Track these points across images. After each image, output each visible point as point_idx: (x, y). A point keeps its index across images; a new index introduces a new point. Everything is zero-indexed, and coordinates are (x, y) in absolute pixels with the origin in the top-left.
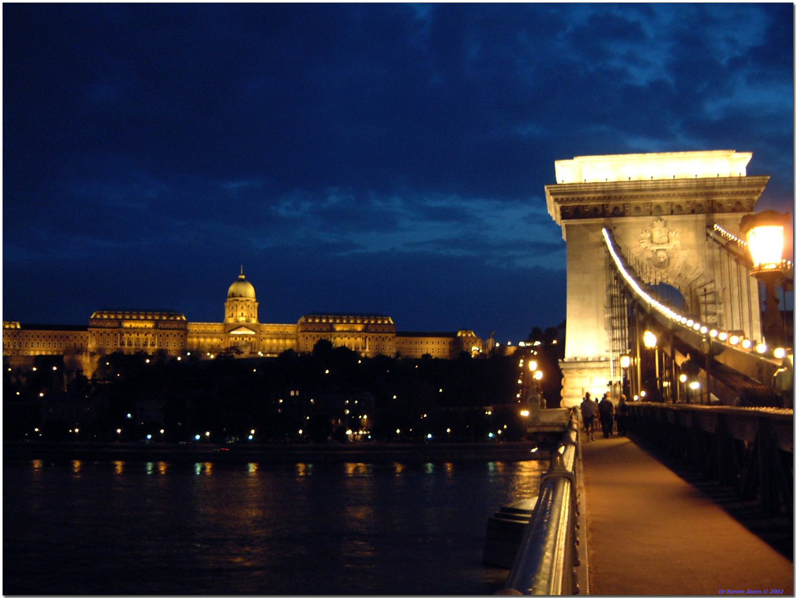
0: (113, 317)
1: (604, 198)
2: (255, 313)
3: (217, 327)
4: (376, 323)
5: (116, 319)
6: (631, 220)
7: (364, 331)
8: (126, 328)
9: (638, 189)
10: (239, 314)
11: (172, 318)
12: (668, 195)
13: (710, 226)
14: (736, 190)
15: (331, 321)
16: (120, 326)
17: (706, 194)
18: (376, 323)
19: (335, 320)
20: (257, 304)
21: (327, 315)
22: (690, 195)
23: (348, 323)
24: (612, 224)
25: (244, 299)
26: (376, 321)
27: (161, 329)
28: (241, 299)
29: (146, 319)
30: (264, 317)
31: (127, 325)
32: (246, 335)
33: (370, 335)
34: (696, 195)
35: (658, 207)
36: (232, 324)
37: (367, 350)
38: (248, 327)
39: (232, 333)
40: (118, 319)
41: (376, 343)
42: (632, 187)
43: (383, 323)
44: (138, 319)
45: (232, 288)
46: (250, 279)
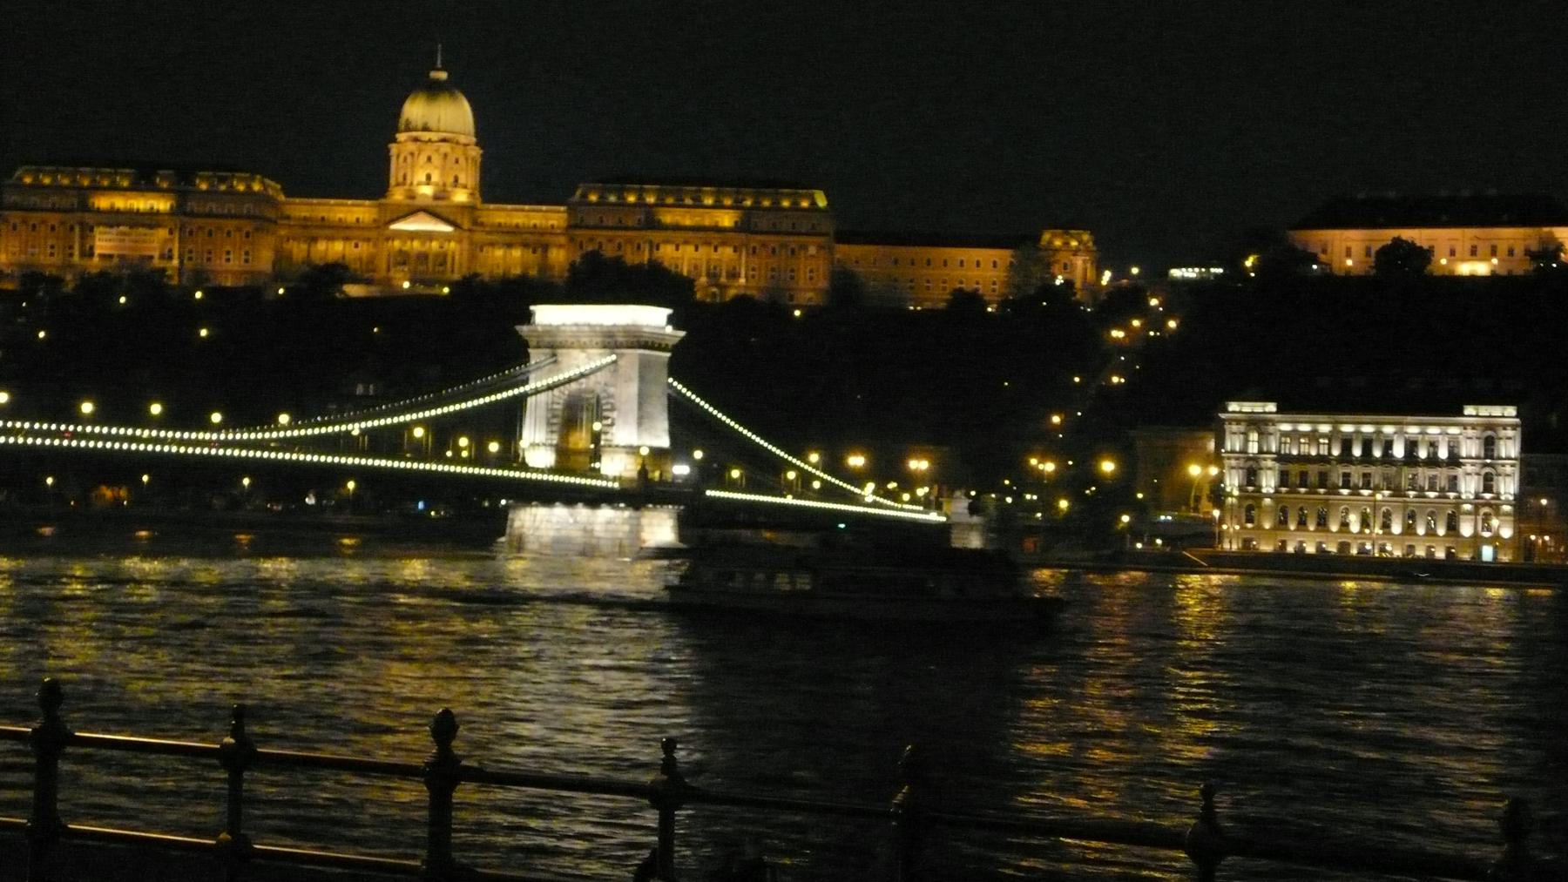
2: (469, 176)
3: (358, 212)
4: (776, 208)
7: (743, 227)
8: (98, 211)
10: (424, 179)
11: (223, 187)
15: (651, 200)
16: (85, 207)
20: (475, 152)
21: (639, 181)
25: (434, 136)
26: (776, 203)
27: (192, 215)
28: (426, 136)
30: (498, 183)
31: (103, 202)
36: (399, 205)
37: (742, 281)
39: (395, 227)
40: (81, 188)
41: (773, 262)
43: (795, 207)
45: (415, 110)
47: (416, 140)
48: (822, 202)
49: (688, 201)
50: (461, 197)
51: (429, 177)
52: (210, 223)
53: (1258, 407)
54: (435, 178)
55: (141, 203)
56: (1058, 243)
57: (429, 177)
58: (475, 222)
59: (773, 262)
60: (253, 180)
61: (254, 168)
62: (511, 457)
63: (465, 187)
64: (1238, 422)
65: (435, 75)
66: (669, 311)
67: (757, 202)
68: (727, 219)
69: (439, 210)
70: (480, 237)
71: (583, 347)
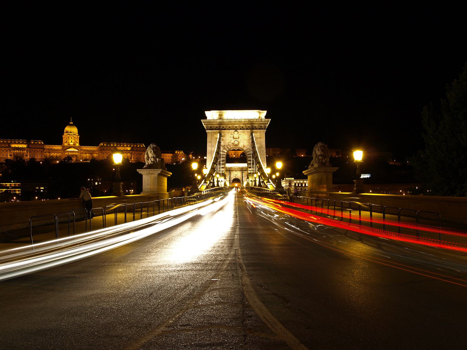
1: (219, 124)
3: (59, 147)
4: (137, 147)
5: (7, 143)
6: (227, 131)
9: (230, 122)
10: (71, 142)
11: (36, 143)
12: (239, 124)
13: (252, 134)
14: (260, 123)
16: (9, 147)
17: (251, 124)
21: (113, 141)
22: (246, 124)
24: (221, 132)
25: (72, 134)
26: (137, 146)
27: (30, 148)
28: (71, 134)
29: (23, 143)
30: (82, 143)
31: (13, 146)
32: (73, 152)
33: (134, 152)
34: (248, 124)
35: (236, 127)
37: (133, 159)
38: (74, 148)
39: (67, 150)
42: (228, 121)
44: (19, 143)
45: (67, 129)
46: (75, 124)
47: (69, 134)
48: (144, 146)
51: (72, 141)
52: (34, 150)
53: (291, 179)
55: (21, 146)
56: (178, 153)
57: (72, 141)
63: (78, 143)
64: (288, 181)
68: (129, 149)
69: (75, 147)
70: (81, 152)
71: (236, 171)
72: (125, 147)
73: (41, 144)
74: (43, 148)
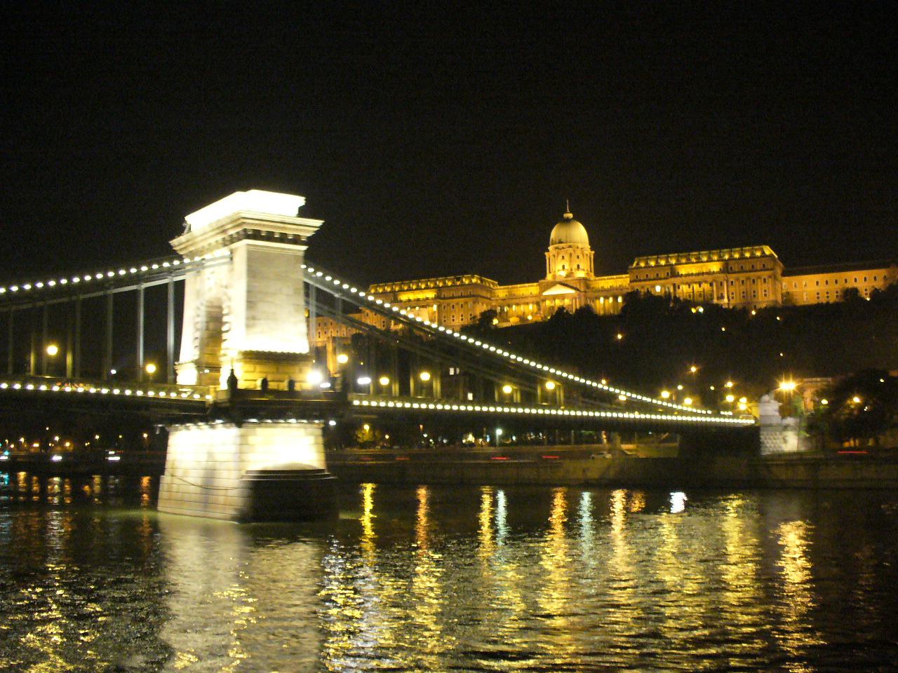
0: (388, 289)
3: (530, 289)
4: (742, 258)
5: (393, 292)
7: (726, 269)
10: (561, 268)
11: (458, 283)
15: (674, 262)
18: (742, 258)
19: (678, 260)
21: (664, 250)
23: (699, 261)
27: (444, 298)
29: (427, 288)
30: (604, 266)
32: (562, 297)
33: (732, 277)
41: (743, 288)
44: (419, 289)
46: (577, 218)
48: (768, 250)
49: (694, 260)
50: (581, 274)
51: (563, 267)
54: (566, 268)
55: (421, 295)
57: (563, 267)
58: (588, 287)
59: (743, 288)
60: (473, 277)
61: (470, 271)
62: (166, 377)
65: (566, 215)
66: (300, 201)
67: (731, 256)
72: (702, 262)
73: (471, 284)
74: (473, 296)
